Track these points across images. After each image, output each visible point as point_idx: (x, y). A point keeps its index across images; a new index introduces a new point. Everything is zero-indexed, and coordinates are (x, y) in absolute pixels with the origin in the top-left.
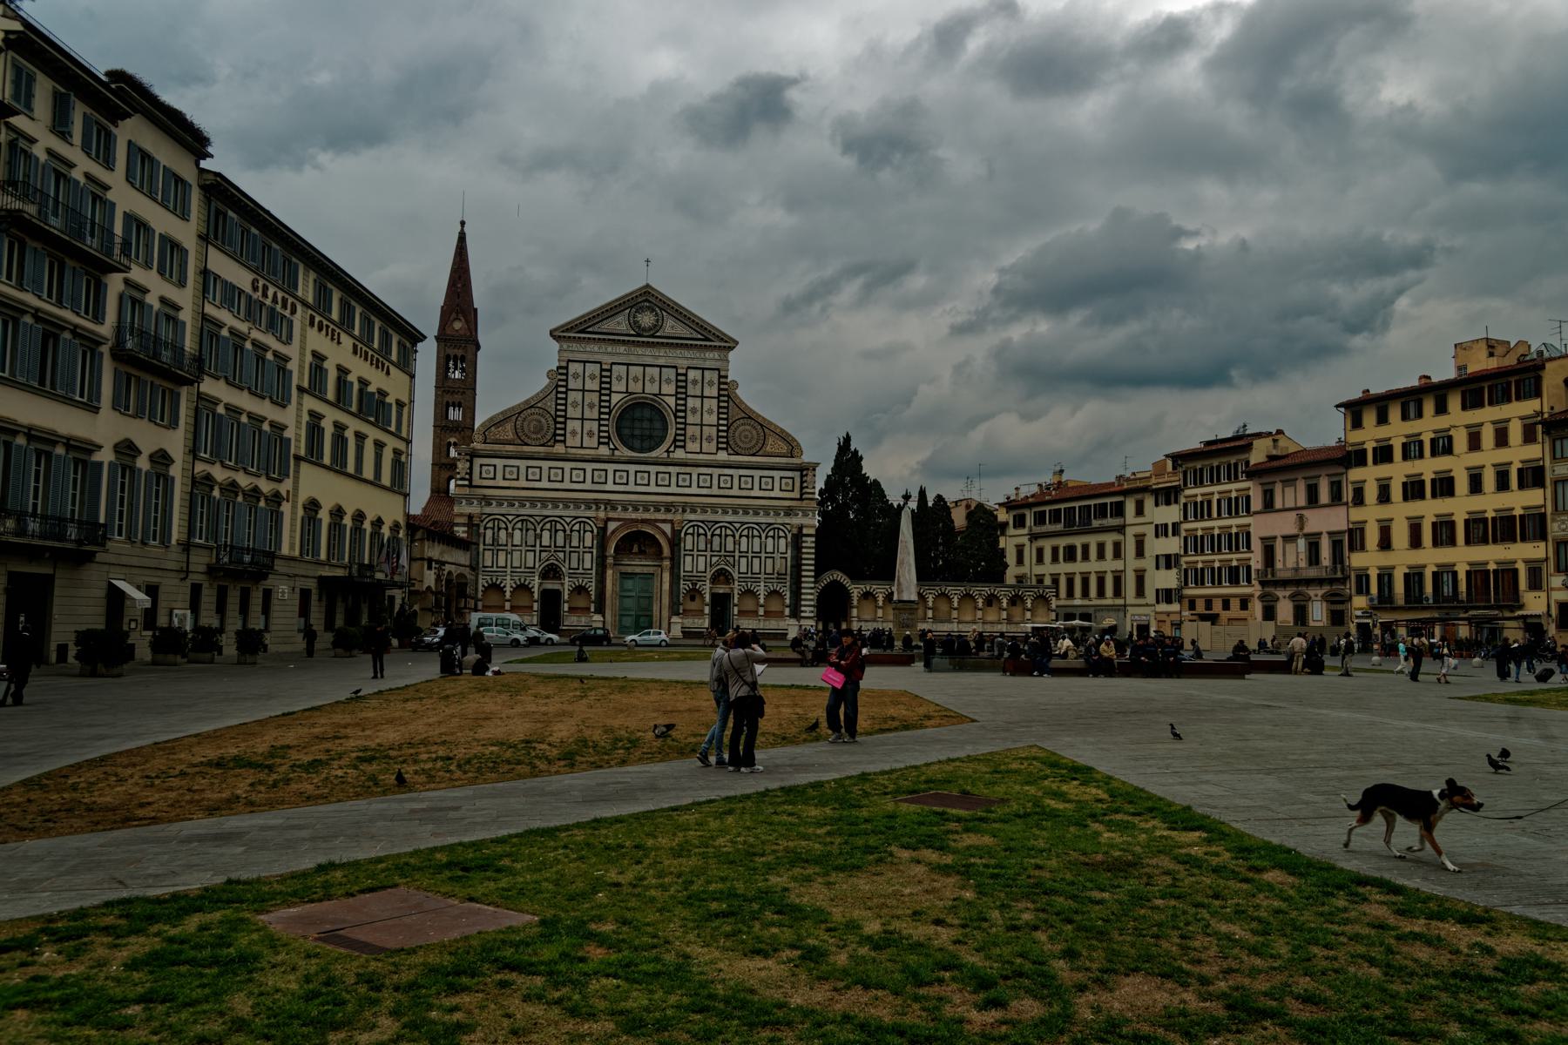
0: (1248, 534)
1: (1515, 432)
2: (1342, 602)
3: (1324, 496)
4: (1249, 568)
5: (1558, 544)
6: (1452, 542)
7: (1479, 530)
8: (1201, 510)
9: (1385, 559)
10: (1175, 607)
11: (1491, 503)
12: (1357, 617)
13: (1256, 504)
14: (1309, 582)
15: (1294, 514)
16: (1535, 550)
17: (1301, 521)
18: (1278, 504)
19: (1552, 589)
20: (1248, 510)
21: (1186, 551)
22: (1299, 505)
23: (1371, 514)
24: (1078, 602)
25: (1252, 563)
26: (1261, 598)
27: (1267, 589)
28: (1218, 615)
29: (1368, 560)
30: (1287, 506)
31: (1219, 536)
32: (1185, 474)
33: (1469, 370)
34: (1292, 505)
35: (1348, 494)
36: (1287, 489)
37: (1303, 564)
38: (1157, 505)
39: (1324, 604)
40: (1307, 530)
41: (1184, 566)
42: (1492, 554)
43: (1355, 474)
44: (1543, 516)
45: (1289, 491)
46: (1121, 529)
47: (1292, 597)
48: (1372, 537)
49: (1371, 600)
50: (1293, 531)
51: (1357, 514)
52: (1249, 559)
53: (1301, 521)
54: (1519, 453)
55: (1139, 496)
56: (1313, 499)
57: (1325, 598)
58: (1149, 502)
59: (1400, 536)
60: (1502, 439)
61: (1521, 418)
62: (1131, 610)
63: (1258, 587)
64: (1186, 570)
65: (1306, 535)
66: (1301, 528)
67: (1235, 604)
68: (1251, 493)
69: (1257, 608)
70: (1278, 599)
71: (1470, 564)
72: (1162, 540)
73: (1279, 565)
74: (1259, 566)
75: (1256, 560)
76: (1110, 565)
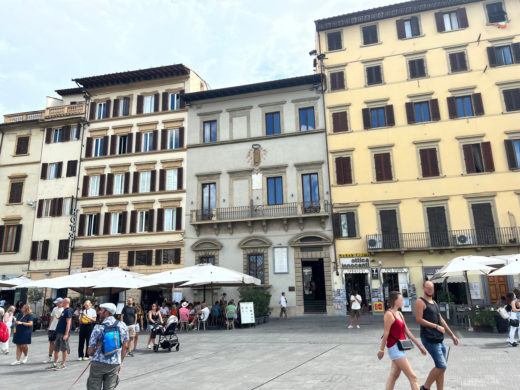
0: (180, 171)
6: (490, 168)
12: (344, 267)
18: (223, 135)
21: (85, 192)
22: (254, 135)
25: (183, 205)
27: (203, 237)
30: (236, 137)
32: (93, 105)
34: (244, 136)
36: (234, 119)
38: (48, 141)
39: (292, 251)
41: (81, 212)
45: (239, 123)
52: (180, 200)
55: (23, 133)
57: (292, 245)
64: (83, 217)
65: (263, 169)
66: (257, 162)
68: (185, 125)
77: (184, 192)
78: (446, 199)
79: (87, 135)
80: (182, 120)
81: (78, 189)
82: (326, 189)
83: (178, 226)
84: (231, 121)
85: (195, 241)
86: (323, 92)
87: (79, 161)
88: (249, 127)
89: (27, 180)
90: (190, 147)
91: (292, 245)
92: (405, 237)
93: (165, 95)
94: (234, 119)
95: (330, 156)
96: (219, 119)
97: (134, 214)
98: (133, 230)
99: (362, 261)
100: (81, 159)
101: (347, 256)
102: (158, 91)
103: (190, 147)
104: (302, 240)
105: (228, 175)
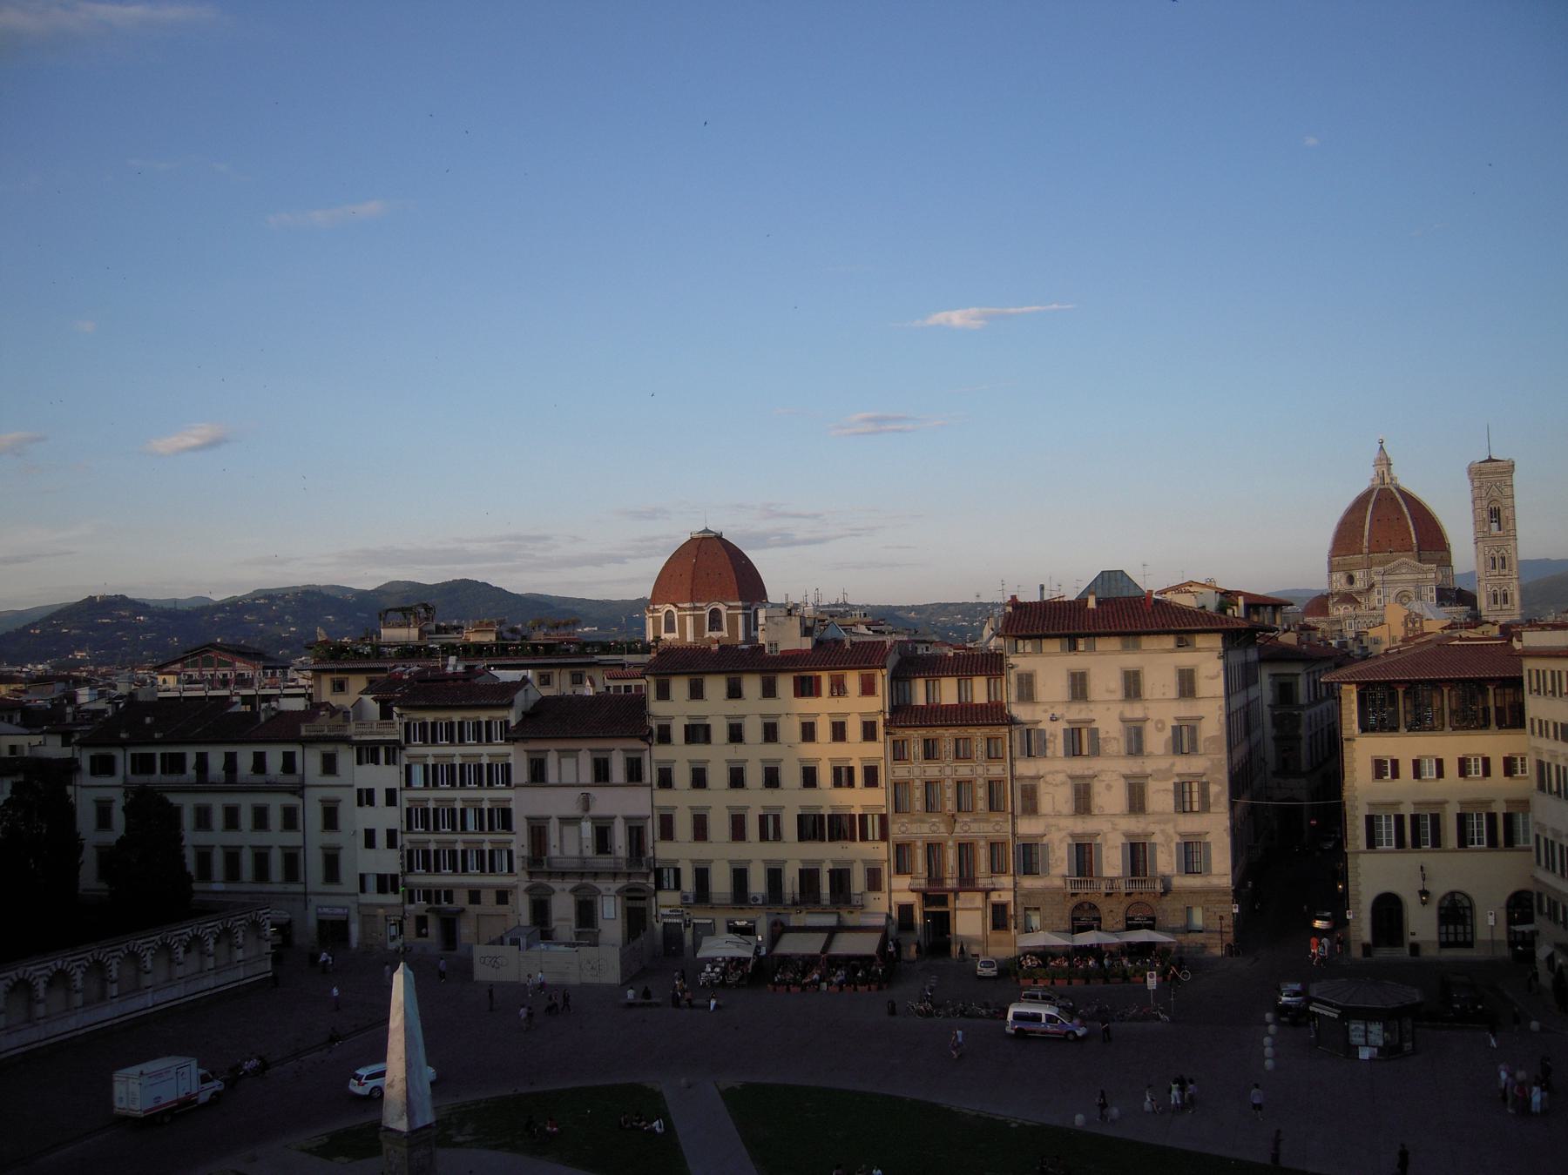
1: (854, 730)
2: (644, 899)
3: (618, 772)
4: (510, 853)
5: (897, 845)
7: (813, 827)
8: (434, 776)
9: (701, 851)
10: (391, 898)
11: (831, 799)
12: (664, 916)
13: (520, 773)
14: (596, 875)
15: (578, 792)
16: (879, 851)
17: (586, 802)
18: (552, 776)
19: (895, 891)
20: (508, 783)
21: (409, 827)
23: (682, 800)
24: (218, 886)
25: (513, 847)
26: (529, 890)
27: (536, 880)
28: (463, 910)
29: (680, 851)
30: (565, 780)
31: (463, 811)
33: (784, 646)
34: (573, 780)
35: (650, 774)
36: (563, 760)
37: (589, 852)
38: (359, 762)
39: (619, 899)
40: (595, 811)
41: (408, 846)
42: (827, 854)
43: (660, 753)
44: (883, 819)
45: (568, 764)
46: (299, 790)
47: (574, 891)
48: (683, 827)
49: (685, 898)
50: (572, 810)
51: (664, 798)
52: (510, 842)
53: (586, 802)
54: (856, 752)
55: (329, 748)
56: (602, 773)
58: (346, 757)
59: (719, 826)
60: (839, 732)
61: (861, 714)
62: (315, 901)
63: (524, 876)
65: (594, 819)
67: (489, 898)
68: (511, 760)
69: (522, 907)
70: (554, 892)
71: (803, 861)
72: (367, 808)
73: (554, 852)
74: (525, 852)
75: (519, 841)
76: (276, 838)
77: (514, 834)
78: (749, 861)
79: (405, 761)
80: (509, 755)
81: (402, 821)
82: (651, 844)
83: (510, 869)
84: (559, 763)
85: (528, 884)
86: (650, 745)
87: (398, 789)
88: (578, 774)
89: (340, 804)
90: (516, 786)
91: (619, 892)
92: (713, 896)
93: (488, 723)
94: (563, 760)
95: (655, 811)
96: (547, 755)
97: (464, 852)
98: (465, 869)
99: (678, 911)
100: (401, 789)
101: (665, 906)
102: (479, 717)
103: (516, 786)
104: (629, 890)
105: (557, 821)
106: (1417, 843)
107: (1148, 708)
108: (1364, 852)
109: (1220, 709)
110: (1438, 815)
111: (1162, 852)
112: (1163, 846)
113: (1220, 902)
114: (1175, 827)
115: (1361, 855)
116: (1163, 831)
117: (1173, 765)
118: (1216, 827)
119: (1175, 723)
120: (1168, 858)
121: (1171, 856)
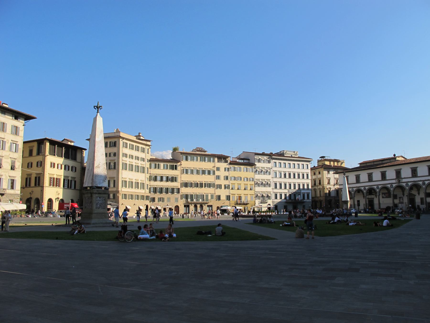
106: (56, 186)
107: (5, 135)
108: (47, 187)
109: (22, 140)
110: (60, 179)
111: (4, 182)
112: (5, 179)
113: (18, 199)
114: (8, 174)
115: (46, 187)
116: (5, 175)
117: (10, 154)
118: (17, 175)
119: (11, 142)
120: (6, 184)
121: (6, 183)
